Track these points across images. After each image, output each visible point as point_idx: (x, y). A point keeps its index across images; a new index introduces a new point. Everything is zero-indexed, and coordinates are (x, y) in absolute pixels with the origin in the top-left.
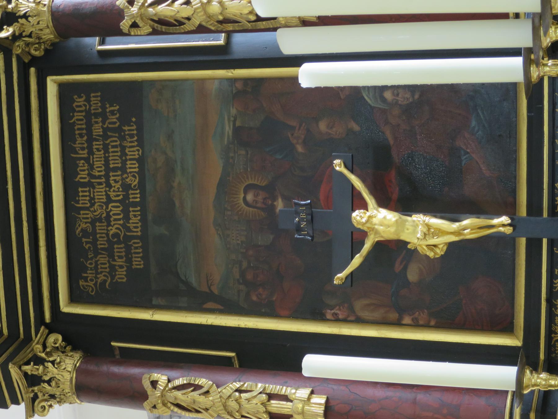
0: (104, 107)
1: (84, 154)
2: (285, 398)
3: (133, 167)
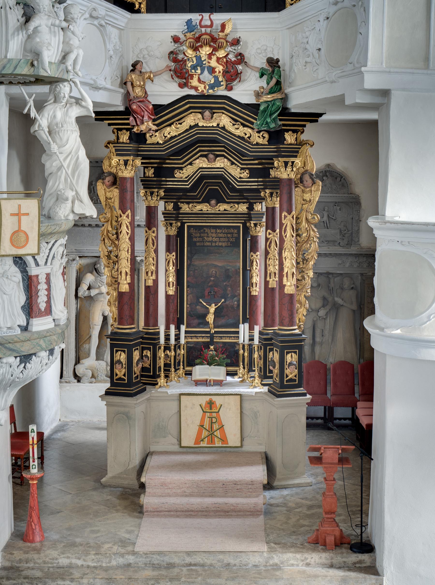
0: (234, 237)
1: (223, 232)
2: (173, 286)
3: (220, 244)
